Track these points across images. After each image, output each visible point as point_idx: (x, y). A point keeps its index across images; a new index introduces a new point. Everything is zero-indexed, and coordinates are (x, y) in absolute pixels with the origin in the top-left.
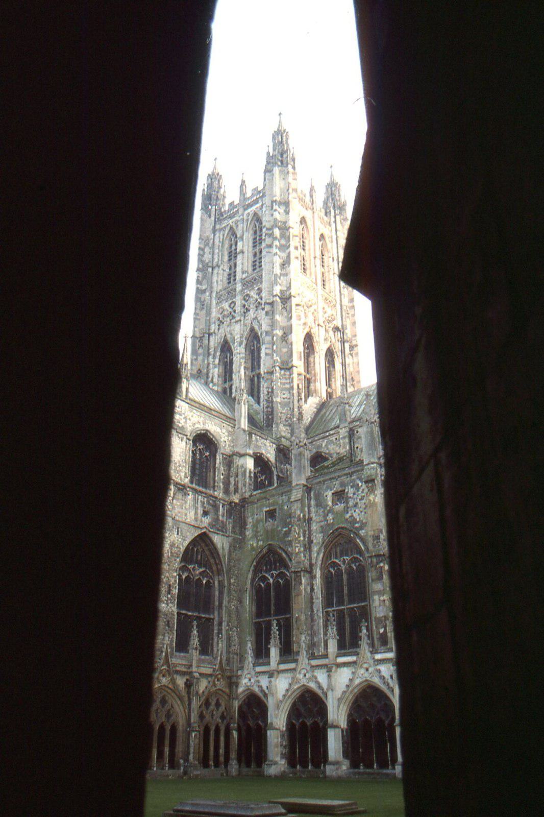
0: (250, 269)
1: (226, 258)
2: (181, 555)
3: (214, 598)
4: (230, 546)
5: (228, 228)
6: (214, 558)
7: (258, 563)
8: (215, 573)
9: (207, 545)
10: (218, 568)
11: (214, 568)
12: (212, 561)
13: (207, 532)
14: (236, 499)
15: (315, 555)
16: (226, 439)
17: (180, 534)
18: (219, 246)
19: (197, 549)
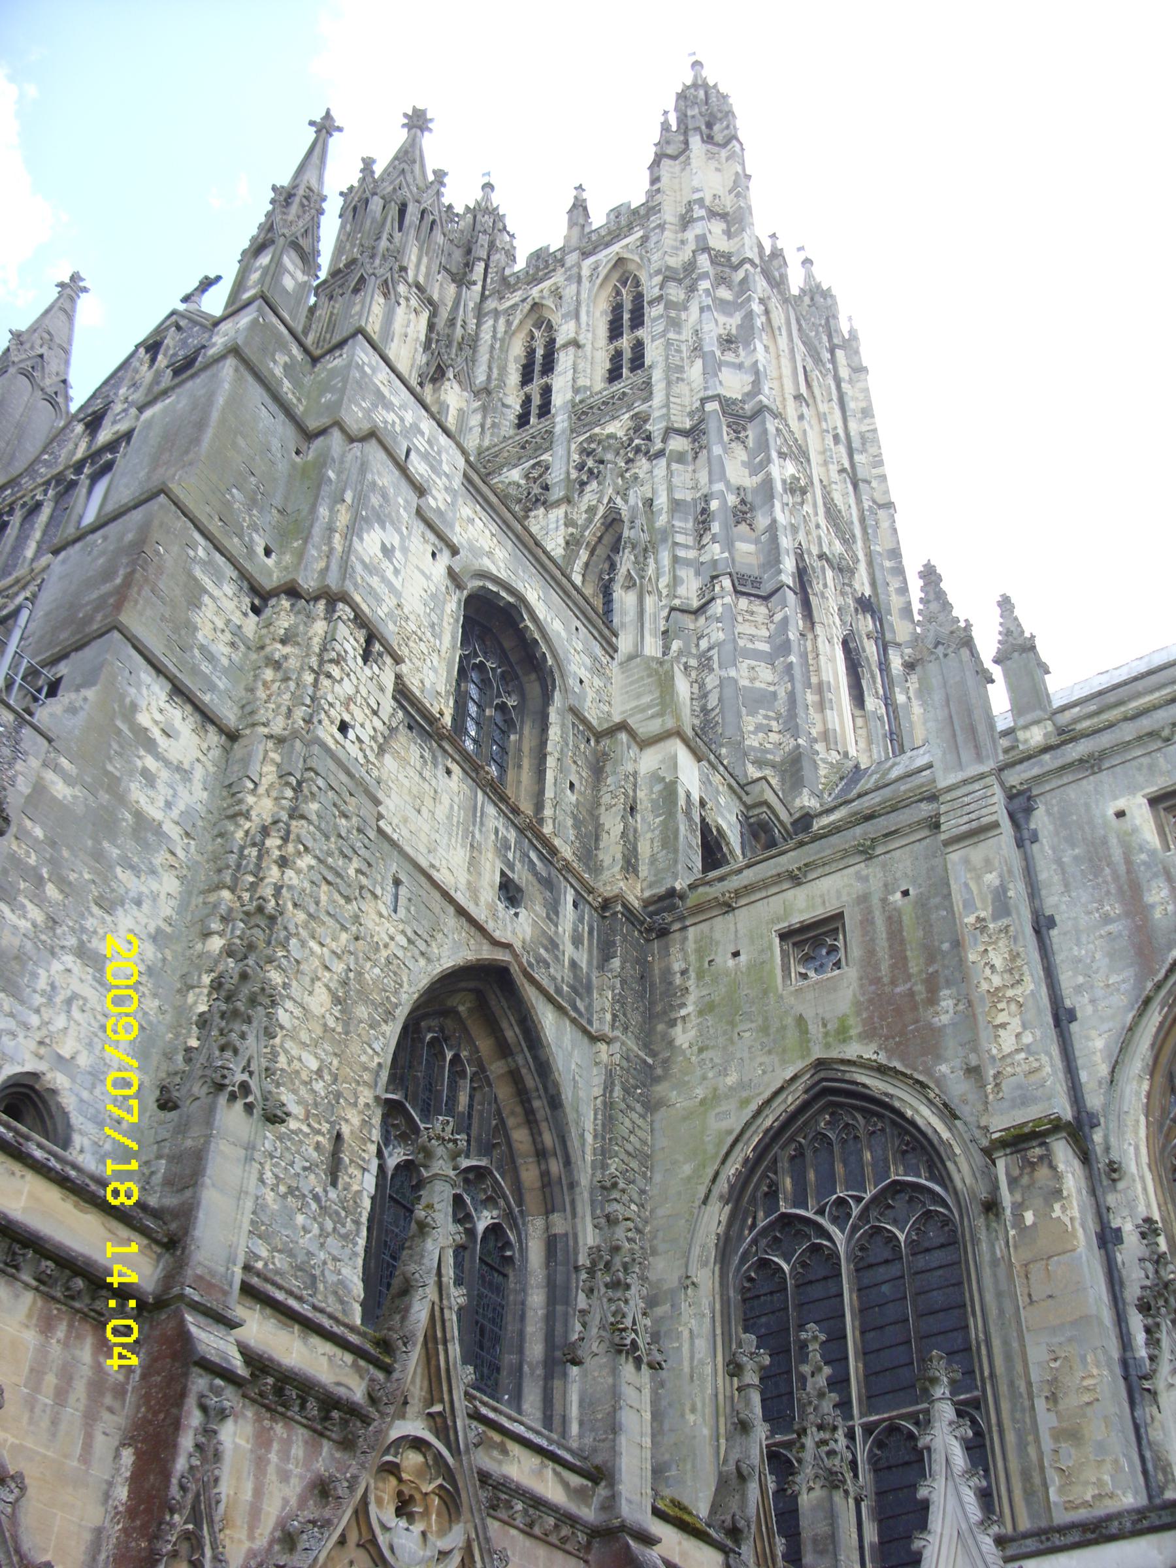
0: (599, 384)
1: (514, 377)
2: (402, 1013)
3: (523, 1318)
4: (608, 1087)
5: (527, 306)
6: (530, 1120)
7: (751, 1166)
8: (532, 1200)
9: (504, 1050)
10: (545, 1174)
11: (530, 1175)
12: (520, 1136)
13: (515, 969)
14: (635, 893)
15: (1104, 1070)
16: (583, 673)
17: (402, 912)
18: (492, 347)
19: (456, 1059)
